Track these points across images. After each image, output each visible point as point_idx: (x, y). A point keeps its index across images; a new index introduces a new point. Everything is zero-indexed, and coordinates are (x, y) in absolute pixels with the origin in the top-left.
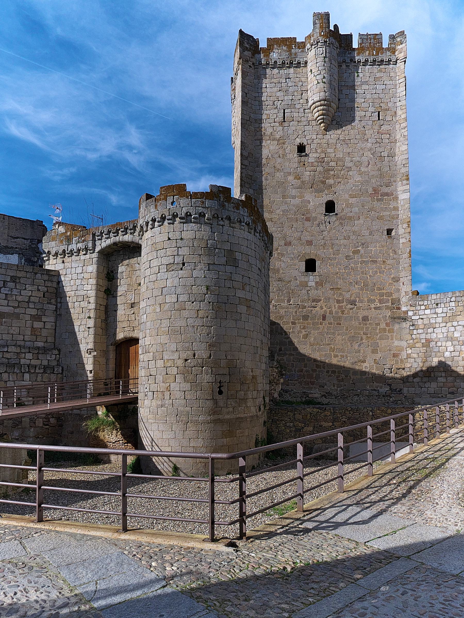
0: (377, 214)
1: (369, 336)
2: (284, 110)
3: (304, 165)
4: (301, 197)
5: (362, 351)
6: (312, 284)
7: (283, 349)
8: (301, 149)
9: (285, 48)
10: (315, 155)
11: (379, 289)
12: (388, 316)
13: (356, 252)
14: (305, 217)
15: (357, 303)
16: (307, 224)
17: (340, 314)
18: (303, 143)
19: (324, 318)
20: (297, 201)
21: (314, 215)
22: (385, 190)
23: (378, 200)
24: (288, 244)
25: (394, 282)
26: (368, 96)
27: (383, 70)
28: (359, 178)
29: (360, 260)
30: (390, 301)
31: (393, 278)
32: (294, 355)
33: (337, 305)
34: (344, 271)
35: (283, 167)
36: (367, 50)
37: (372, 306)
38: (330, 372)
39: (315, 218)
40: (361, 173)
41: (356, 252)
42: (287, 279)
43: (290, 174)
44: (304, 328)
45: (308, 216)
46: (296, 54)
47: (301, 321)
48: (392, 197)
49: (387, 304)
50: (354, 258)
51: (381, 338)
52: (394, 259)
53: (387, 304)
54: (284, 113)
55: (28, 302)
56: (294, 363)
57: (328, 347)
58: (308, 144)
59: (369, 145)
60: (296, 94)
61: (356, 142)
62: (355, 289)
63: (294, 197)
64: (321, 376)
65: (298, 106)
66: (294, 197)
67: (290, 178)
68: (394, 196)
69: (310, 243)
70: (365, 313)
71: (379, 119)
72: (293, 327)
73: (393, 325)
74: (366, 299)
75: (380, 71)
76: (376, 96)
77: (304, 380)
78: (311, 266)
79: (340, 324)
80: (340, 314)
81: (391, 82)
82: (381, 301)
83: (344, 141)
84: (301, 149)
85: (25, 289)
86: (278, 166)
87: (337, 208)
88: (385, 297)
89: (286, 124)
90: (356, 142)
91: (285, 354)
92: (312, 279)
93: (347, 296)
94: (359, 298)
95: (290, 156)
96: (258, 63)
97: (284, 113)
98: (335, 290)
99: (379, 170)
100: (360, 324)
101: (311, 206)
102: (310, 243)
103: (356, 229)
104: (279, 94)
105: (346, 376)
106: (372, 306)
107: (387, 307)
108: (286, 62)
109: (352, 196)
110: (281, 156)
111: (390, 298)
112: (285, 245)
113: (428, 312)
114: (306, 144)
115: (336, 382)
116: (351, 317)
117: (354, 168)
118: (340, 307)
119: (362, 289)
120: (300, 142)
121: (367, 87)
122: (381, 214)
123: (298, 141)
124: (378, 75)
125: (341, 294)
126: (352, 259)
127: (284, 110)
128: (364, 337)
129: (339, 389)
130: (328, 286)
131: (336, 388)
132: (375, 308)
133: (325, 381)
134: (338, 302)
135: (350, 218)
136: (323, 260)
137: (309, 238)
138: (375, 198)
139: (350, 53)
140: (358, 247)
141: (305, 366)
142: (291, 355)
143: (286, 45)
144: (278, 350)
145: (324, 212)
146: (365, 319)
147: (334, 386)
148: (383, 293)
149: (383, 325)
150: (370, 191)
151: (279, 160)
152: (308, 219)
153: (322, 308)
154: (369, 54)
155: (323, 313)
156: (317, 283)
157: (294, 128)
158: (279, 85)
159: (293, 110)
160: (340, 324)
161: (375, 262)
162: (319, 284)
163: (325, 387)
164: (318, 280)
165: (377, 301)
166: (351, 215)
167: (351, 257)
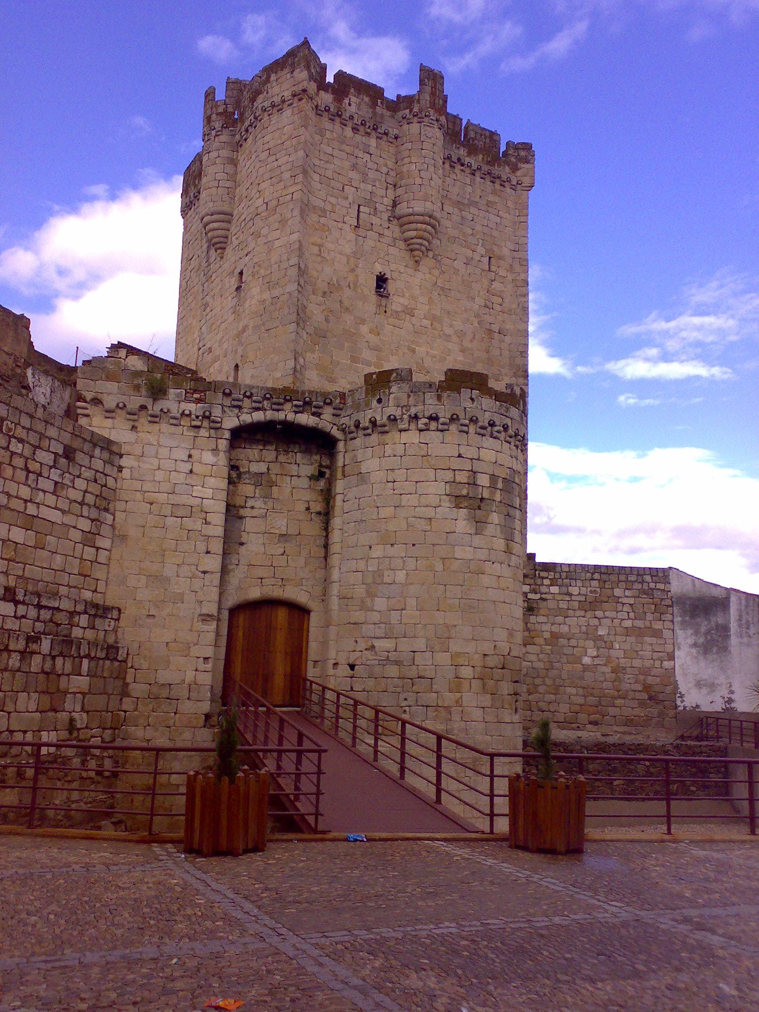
2: (359, 206)
8: (381, 281)
9: (367, 99)
10: (401, 300)
26: (479, 228)
55: (82, 504)
75: (494, 192)
76: (486, 230)
83: (442, 289)
84: (381, 281)
85: (79, 477)
86: (346, 303)
89: (361, 232)
117: (454, 338)
120: (381, 270)
121: (476, 212)
123: (379, 268)
124: (491, 198)
127: (359, 206)
143: (368, 95)
151: (348, 293)
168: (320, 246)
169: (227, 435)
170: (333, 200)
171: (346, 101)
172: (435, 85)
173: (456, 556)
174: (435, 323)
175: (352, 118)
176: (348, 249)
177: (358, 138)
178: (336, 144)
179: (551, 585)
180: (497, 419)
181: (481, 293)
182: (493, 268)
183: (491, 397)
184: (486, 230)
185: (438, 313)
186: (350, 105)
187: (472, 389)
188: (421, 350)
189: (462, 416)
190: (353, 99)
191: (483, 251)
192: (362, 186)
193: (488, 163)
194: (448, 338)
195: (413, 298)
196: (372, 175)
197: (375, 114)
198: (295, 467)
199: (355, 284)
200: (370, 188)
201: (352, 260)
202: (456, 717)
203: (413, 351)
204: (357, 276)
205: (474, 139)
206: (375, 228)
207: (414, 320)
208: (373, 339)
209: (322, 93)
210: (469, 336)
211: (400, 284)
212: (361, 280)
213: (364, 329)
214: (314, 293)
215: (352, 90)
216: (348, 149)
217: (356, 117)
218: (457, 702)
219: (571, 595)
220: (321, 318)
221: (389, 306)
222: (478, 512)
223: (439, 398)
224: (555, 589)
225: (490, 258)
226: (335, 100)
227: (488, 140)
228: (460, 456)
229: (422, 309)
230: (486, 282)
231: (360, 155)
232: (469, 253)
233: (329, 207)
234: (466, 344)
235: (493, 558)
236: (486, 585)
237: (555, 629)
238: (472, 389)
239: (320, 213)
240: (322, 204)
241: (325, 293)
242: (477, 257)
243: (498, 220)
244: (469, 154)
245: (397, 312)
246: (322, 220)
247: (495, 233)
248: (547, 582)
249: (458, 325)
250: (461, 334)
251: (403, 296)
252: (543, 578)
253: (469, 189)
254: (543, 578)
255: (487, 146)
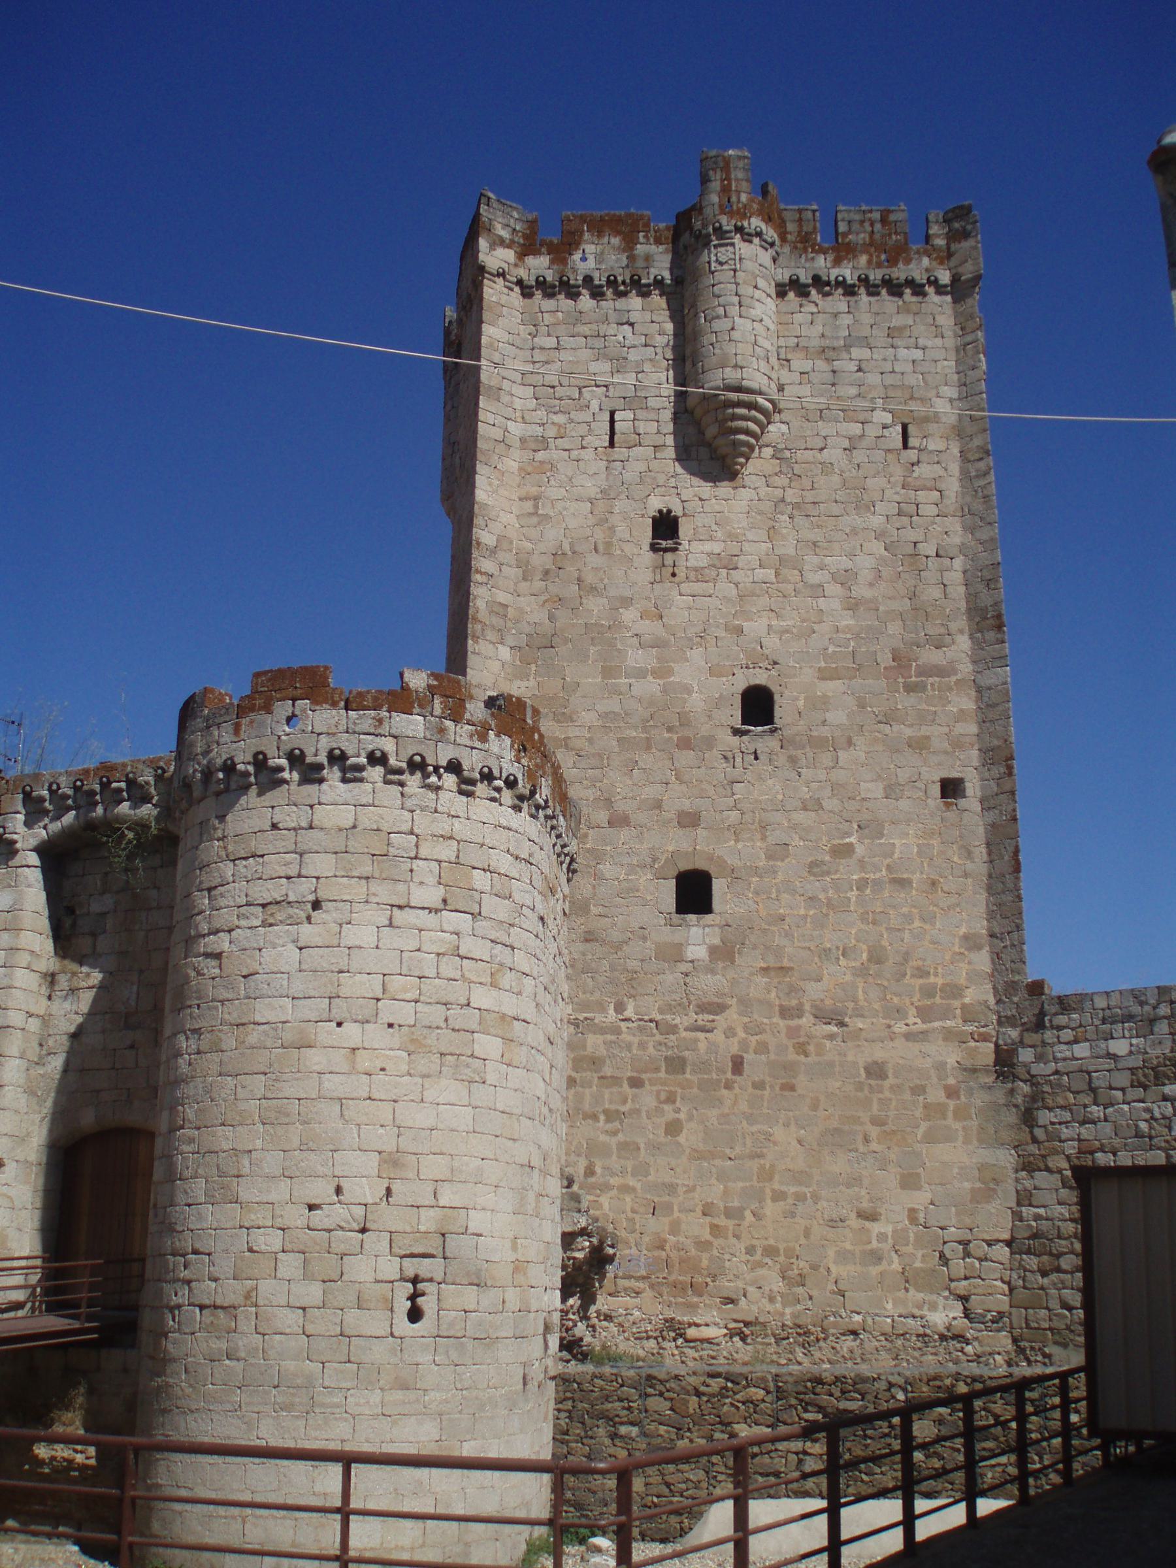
0: (908, 732)
1: (890, 1127)
2: (612, 414)
3: (674, 575)
4: (661, 672)
5: (866, 1182)
6: (697, 951)
7: (598, 1170)
8: (665, 527)
9: (616, 241)
10: (708, 547)
11: (922, 973)
12: (951, 1061)
13: (843, 851)
14: (675, 737)
15: (847, 1019)
16: (686, 758)
17: (792, 1056)
18: (669, 511)
19: (738, 1065)
20: (650, 687)
21: (705, 730)
22: (931, 656)
23: (910, 688)
24: (619, 821)
25: (969, 949)
27: (914, 308)
28: (848, 621)
29: (855, 877)
30: (958, 1012)
31: (966, 937)
32: (634, 1189)
33: (782, 1023)
34: (802, 912)
35: (606, 581)
36: (862, 252)
37: (900, 1028)
38: (759, 1251)
39: (710, 742)
40: (852, 605)
41: (843, 851)
42: (615, 936)
43: (627, 602)
44: (671, 1099)
45: (688, 733)
46: (648, 258)
47: (662, 1074)
48: (953, 679)
49: (949, 1023)
50: (836, 871)
51: (930, 1138)
52: (966, 875)
53: (949, 1023)
54: (612, 422)
56: (637, 1217)
57: (754, 1165)
58: (685, 515)
59: (877, 521)
60: (647, 367)
61: (836, 509)
62: (838, 973)
63: (641, 674)
64: (727, 1264)
65: (652, 402)
66: (641, 674)
67: (629, 616)
68: (959, 676)
69: (689, 820)
70: (879, 1053)
71: (905, 446)
72: (635, 1096)
73: (970, 1092)
74: (877, 1006)
77: (672, 1278)
78: (694, 893)
79: (792, 1088)
80: (792, 1056)
81: (938, 342)
82: (925, 1014)
83: (796, 506)
86: (589, 578)
87: (782, 712)
88: (938, 1000)
89: (619, 452)
90: (836, 509)
91: (606, 1187)
92: (698, 936)
93: (814, 991)
94: (855, 1000)
95: (629, 549)
96: (533, 278)
97: (612, 422)
98: (772, 973)
99: (913, 596)
100: (859, 1087)
101: (696, 702)
102: (689, 820)
103: (839, 775)
104: (594, 367)
105: (815, 1267)
106: (900, 1028)
107: (949, 1035)
108: (620, 279)
109: (825, 675)
110: (601, 548)
111: (956, 1003)
112: (611, 824)
113: (1082, 1050)
114: (680, 514)
115: (777, 1285)
116: (831, 1064)
117: (833, 589)
118: (792, 1032)
119: (862, 972)
120: (661, 506)
121: (865, 353)
122: (922, 733)
123: (656, 504)
124: (898, 321)
125: (792, 990)
126: (828, 873)
127: (612, 414)
128: (874, 1131)
129: (788, 1311)
130: (749, 960)
131: (778, 1306)
132: (909, 1036)
133: (740, 1284)
134: (784, 1012)
135: (820, 744)
136: (733, 874)
137: (686, 805)
138: (901, 680)
139: (813, 259)
140: (848, 834)
141: (675, 1229)
142: (625, 1189)
143: (617, 233)
144: (582, 1172)
145: (737, 721)
146: (876, 1071)
147: (772, 1300)
148: (934, 986)
149: (936, 1095)
150: (886, 659)
151: (594, 560)
152: (685, 744)
153: (730, 1032)
154: (869, 262)
155: (735, 1049)
156: (713, 950)
157: (642, 466)
158: (598, 343)
159: (641, 414)
160: (792, 1088)
161: (902, 883)
162: (723, 953)
163: (743, 1302)
164: (717, 941)
165: (912, 1011)
166: (825, 732)
167: (825, 868)
168: (536, 499)
169: (34, 859)
170: (560, 419)
171: (577, 256)
172: (728, 179)
173: (258, 1019)
174: (784, 571)
175: (588, 279)
176: (590, 488)
177: (607, 305)
178: (561, 330)
179: (1076, 1041)
180: (347, 744)
181: (889, 493)
182: (913, 442)
183: (334, 704)
184: (889, 380)
185: (792, 552)
186: (584, 259)
187: (294, 700)
188: (755, 627)
189: (271, 751)
190: (590, 248)
191: (887, 418)
192: (617, 379)
193: (879, 265)
194: (818, 590)
195: (732, 537)
196: (633, 356)
197: (632, 258)
198: (153, 893)
199: (608, 545)
200: (631, 379)
201: (601, 505)
202: (246, 1325)
203: (739, 631)
204: (612, 529)
205: (845, 235)
206: (646, 440)
207: (737, 575)
208: (649, 627)
209: (531, 261)
210: (866, 575)
211: (700, 520)
212: (622, 531)
213: (629, 616)
214: (525, 579)
215: (587, 236)
216: (586, 329)
217: (596, 275)
218: (247, 1296)
219: (1114, 1057)
220: (540, 616)
221: (681, 562)
222: (306, 929)
223: (237, 729)
224: (1082, 1050)
225: (905, 428)
226: (552, 262)
227: (878, 226)
228: (274, 826)
229: (756, 548)
230: (898, 472)
231: (612, 329)
232: (856, 429)
233: (551, 432)
234: (861, 591)
235: (337, 1015)
236: (317, 1068)
237: (1086, 1132)
238: (294, 700)
239: (534, 446)
240: (539, 430)
241: (547, 572)
242: (872, 431)
243: (918, 354)
244: (837, 262)
245: (696, 569)
246: (540, 456)
247: (913, 380)
248: (1067, 1035)
249: (837, 562)
250: (845, 579)
251: (711, 539)
252: (1059, 1028)
253: (846, 320)
254: (1059, 1028)
255: (877, 236)
